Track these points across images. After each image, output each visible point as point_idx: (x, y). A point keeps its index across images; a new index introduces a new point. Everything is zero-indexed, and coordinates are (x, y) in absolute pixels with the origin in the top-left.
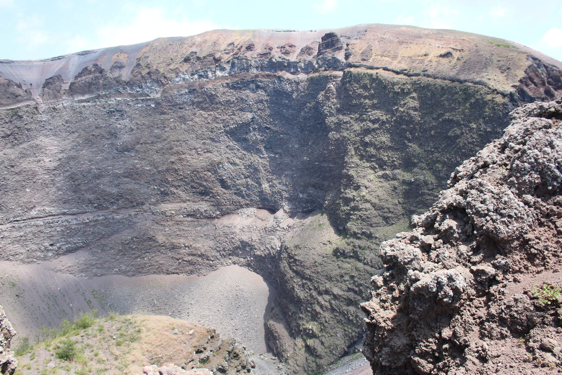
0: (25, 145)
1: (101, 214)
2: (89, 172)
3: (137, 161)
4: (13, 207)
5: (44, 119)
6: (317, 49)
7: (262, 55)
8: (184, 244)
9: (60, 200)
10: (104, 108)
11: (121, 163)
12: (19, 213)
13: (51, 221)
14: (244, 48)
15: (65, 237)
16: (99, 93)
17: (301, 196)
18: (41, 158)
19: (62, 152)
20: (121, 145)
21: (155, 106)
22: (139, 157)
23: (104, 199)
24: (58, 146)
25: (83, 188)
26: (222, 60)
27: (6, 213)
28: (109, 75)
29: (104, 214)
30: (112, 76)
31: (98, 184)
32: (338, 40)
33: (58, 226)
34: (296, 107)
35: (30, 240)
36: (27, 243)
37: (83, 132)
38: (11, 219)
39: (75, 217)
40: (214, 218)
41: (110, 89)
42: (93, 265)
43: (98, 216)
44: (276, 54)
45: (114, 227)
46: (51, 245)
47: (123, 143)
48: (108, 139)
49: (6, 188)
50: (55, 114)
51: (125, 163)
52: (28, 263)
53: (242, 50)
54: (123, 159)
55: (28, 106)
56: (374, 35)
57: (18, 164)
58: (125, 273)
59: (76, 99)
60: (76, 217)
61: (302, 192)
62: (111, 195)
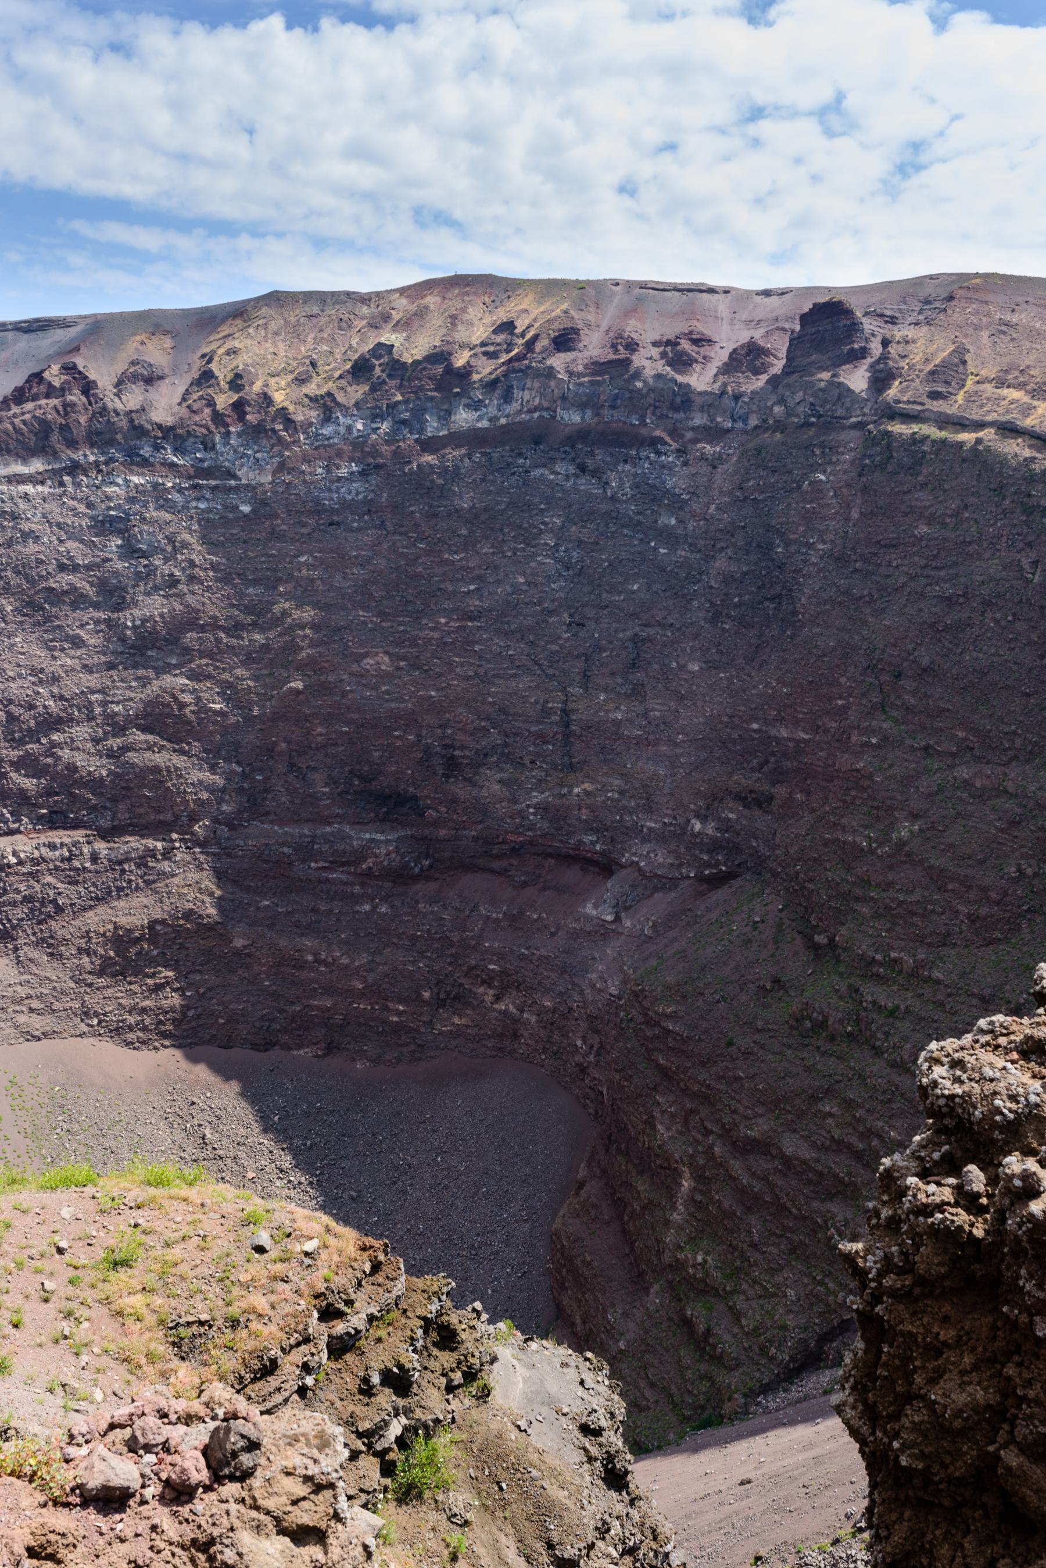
1: (58, 841)
2: (32, 707)
3: (184, 681)
6: (783, 353)
7: (598, 367)
8: (314, 954)
10: (90, 506)
11: (134, 684)
14: (543, 343)
16: (75, 456)
17: (698, 826)
20: (138, 627)
21: (253, 511)
22: (192, 670)
26: (476, 377)
28: (113, 402)
29: (67, 840)
30: (119, 406)
31: (53, 745)
32: (854, 328)
34: (702, 542)
37: (15, 580)
40: (416, 878)
41: (112, 446)
44: (647, 363)
47: (144, 621)
48: (96, 606)
51: (144, 686)
53: (539, 346)
54: (141, 672)
56: (976, 313)
58: (117, 1031)
61: (703, 818)
62: (94, 784)
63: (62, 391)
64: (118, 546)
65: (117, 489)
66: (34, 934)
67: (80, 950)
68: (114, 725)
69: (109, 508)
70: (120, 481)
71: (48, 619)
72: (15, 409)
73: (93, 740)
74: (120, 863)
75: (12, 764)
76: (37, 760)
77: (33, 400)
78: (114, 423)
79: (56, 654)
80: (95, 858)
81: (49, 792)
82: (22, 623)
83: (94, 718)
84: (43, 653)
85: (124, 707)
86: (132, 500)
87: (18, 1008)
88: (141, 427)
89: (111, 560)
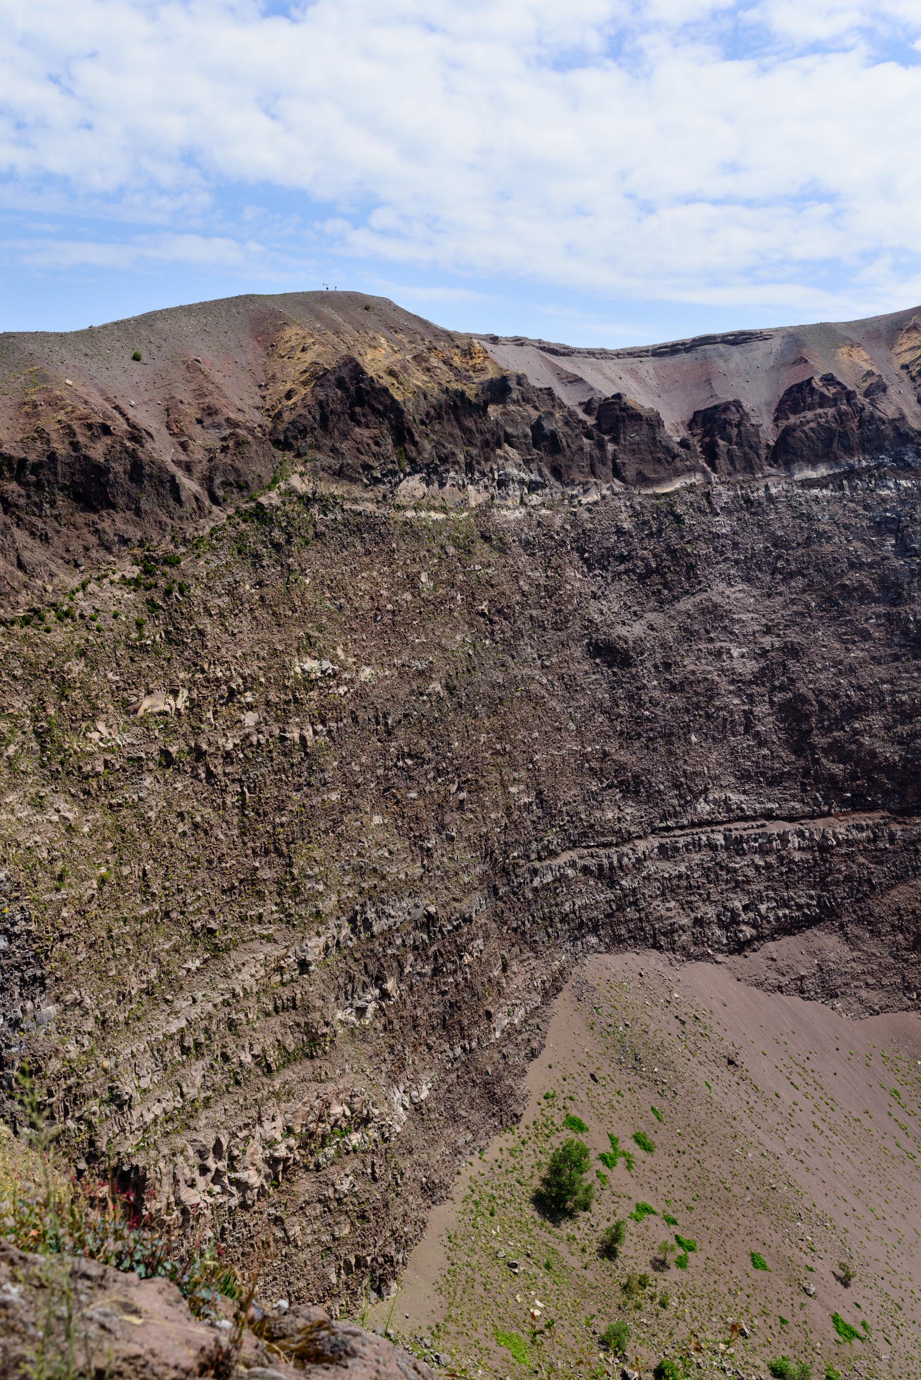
0: (686, 604)
1: (864, 823)
2: (836, 697)
4: (662, 787)
5: (724, 531)
9: (763, 774)
10: (867, 507)
11: (916, 675)
12: (674, 807)
13: (744, 833)
15: (776, 885)
16: (851, 462)
18: (724, 644)
19: (768, 630)
23: (870, 779)
24: (755, 611)
25: (820, 741)
27: (646, 803)
29: (871, 822)
31: (856, 732)
33: (755, 853)
35: (699, 888)
36: (693, 898)
38: (658, 824)
39: (795, 826)
42: (858, 980)
43: (860, 828)
45: (894, 864)
46: (746, 908)
48: (876, 600)
49: (651, 730)
50: (748, 516)
52: (697, 958)
55: (691, 488)
57: (679, 659)
59: (798, 476)
60: (802, 828)
62: (890, 769)
63: (834, 401)
64: (893, 546)
65: (887, 492)
66: (855, 912)
67: (893, 926)
68: (902, 713)
69: (886, 510)
70: (891, 484)
71: (842, 612)
72: (793, 420)
73: (885, 728)
74: (913, 843)
75: (823, 750)
76: (843, 747)
77: (809, 410)
78: (882, 431)
79: (850, 646)
80: (892, 839)
81: (854, 777)
82: (821, 618)
83: (884, 707)
84: (837, 645)
85: (909, 695)
86: (903, 502)
87: (857, 983)
88: (907, 434)
89: (887, 558)
